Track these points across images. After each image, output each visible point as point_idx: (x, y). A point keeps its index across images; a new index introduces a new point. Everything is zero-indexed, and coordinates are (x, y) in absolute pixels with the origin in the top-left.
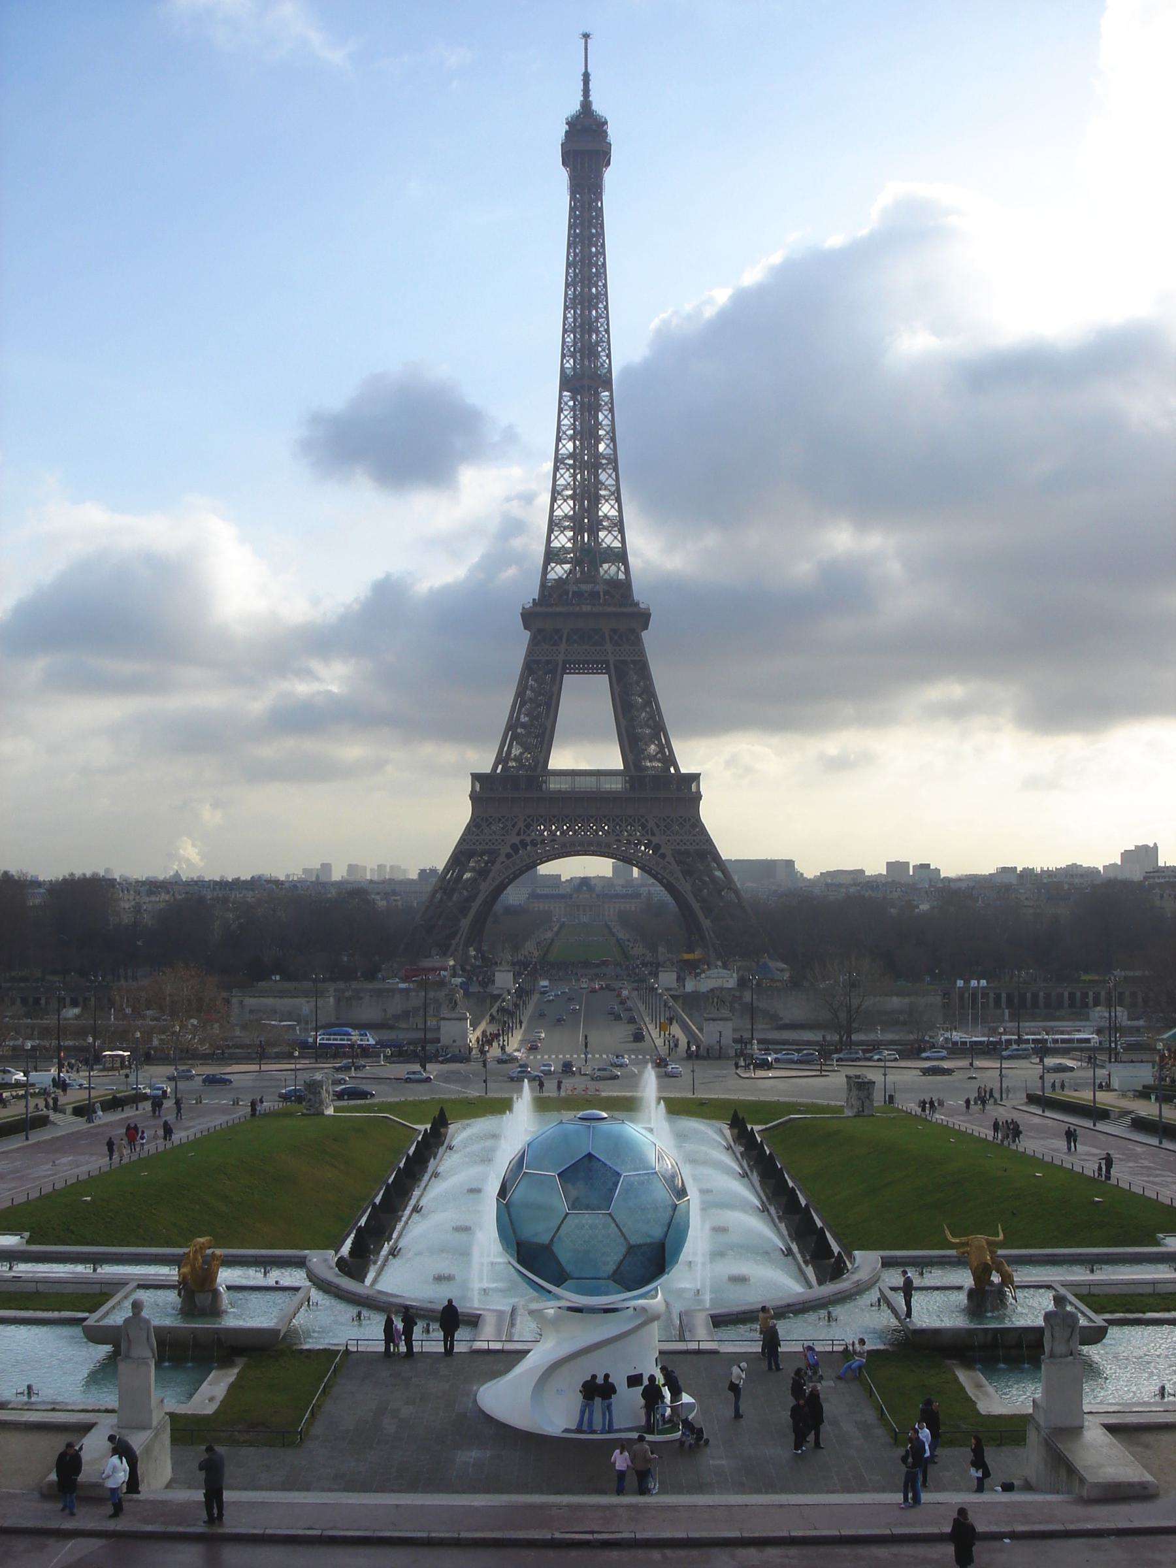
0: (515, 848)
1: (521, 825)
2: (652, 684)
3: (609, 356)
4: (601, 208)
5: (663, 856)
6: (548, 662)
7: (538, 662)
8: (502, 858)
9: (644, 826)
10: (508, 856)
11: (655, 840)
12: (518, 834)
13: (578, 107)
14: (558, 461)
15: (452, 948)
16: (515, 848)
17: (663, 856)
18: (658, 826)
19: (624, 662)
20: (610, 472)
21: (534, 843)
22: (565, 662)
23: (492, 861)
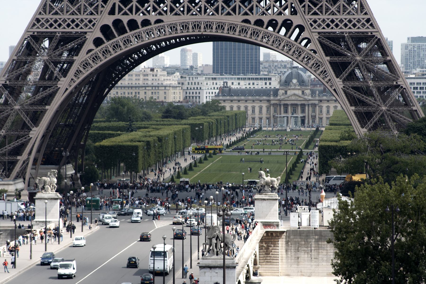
0: (105, 29)
8: (89, 45)
10: (98, 42)
12: (112, 12)
15: (17, 168)
16: (105, 29)
21: (133, 25)
23: (75, 51)
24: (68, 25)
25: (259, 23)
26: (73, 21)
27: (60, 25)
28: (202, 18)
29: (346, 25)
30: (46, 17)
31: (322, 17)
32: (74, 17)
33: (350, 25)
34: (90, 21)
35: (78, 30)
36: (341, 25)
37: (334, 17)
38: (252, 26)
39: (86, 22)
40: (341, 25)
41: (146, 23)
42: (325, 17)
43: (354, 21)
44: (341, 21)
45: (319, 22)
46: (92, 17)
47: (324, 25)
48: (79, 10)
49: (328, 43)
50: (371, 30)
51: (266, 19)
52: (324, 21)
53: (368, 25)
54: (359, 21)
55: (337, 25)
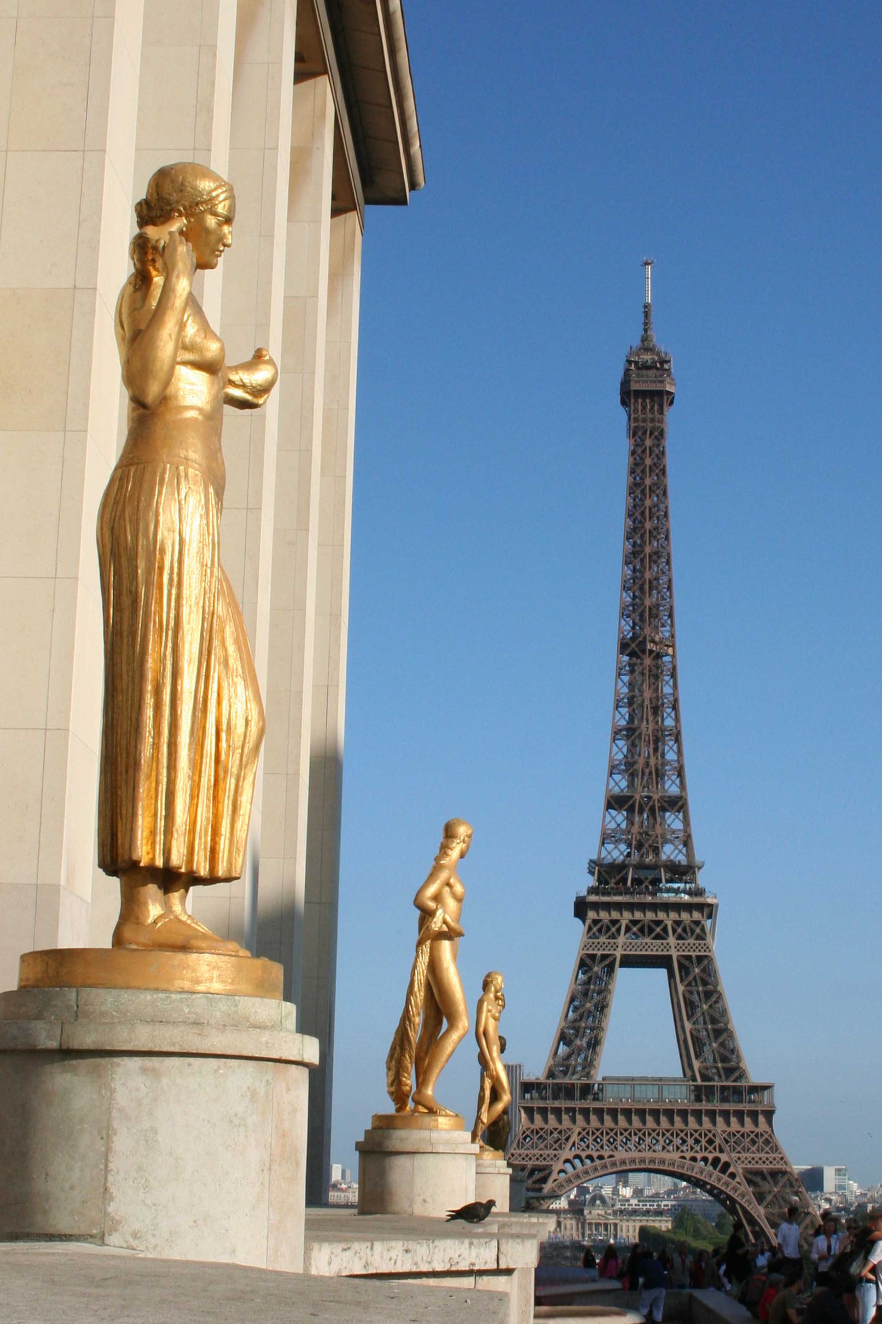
1: (575, 1138)
2: (716, 984)
3: (671, 616)
4: (663, 453)
5: (733, 1176)
6: (604, 957)
7: (593, 957)
8: (554, 1176)
9: (710, 1142)
11: (724, 1158)
13: (636, 342)
14: (616, 733)
17: (733, 1176)
18: (727, 1142)
19: (689, 958)
20: (671, 743)
22: (623, 956)
23: (544, 1180)
24: (538, 1159)
25: (694, 1159)
26: (541, 1156)
27: (530, 1159)
28: (648, 1155)
29: (764, 1162)
30: (519, 1152)
31: (743, 1155)
32: (542, 1152)
33: (767, 1162)
34: (555, 1156)
35: (544, 1163)
36: (760, 1162)
37: (754, 1155)
38: (688, 1162)
39: (552, 1156)
40: (760, 1162)
41: (601, 1157)
42: (747, 1155)
43: (771, 1159)
44: (760, 1159)
45: (742, 1159)
46: (556, 1152)
47: (746, 1162)
48: (546, 1147)
49: (750, 1176)
50: (784, 1167)
51: (699, 1156)
52: (746, 1158)
53: (782, 1162)
54: (775, 1159)
55: (757, 1162)
